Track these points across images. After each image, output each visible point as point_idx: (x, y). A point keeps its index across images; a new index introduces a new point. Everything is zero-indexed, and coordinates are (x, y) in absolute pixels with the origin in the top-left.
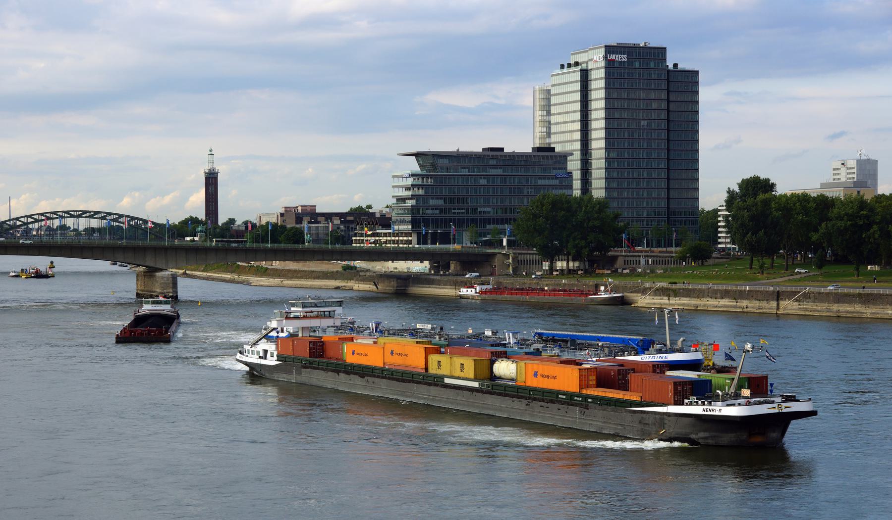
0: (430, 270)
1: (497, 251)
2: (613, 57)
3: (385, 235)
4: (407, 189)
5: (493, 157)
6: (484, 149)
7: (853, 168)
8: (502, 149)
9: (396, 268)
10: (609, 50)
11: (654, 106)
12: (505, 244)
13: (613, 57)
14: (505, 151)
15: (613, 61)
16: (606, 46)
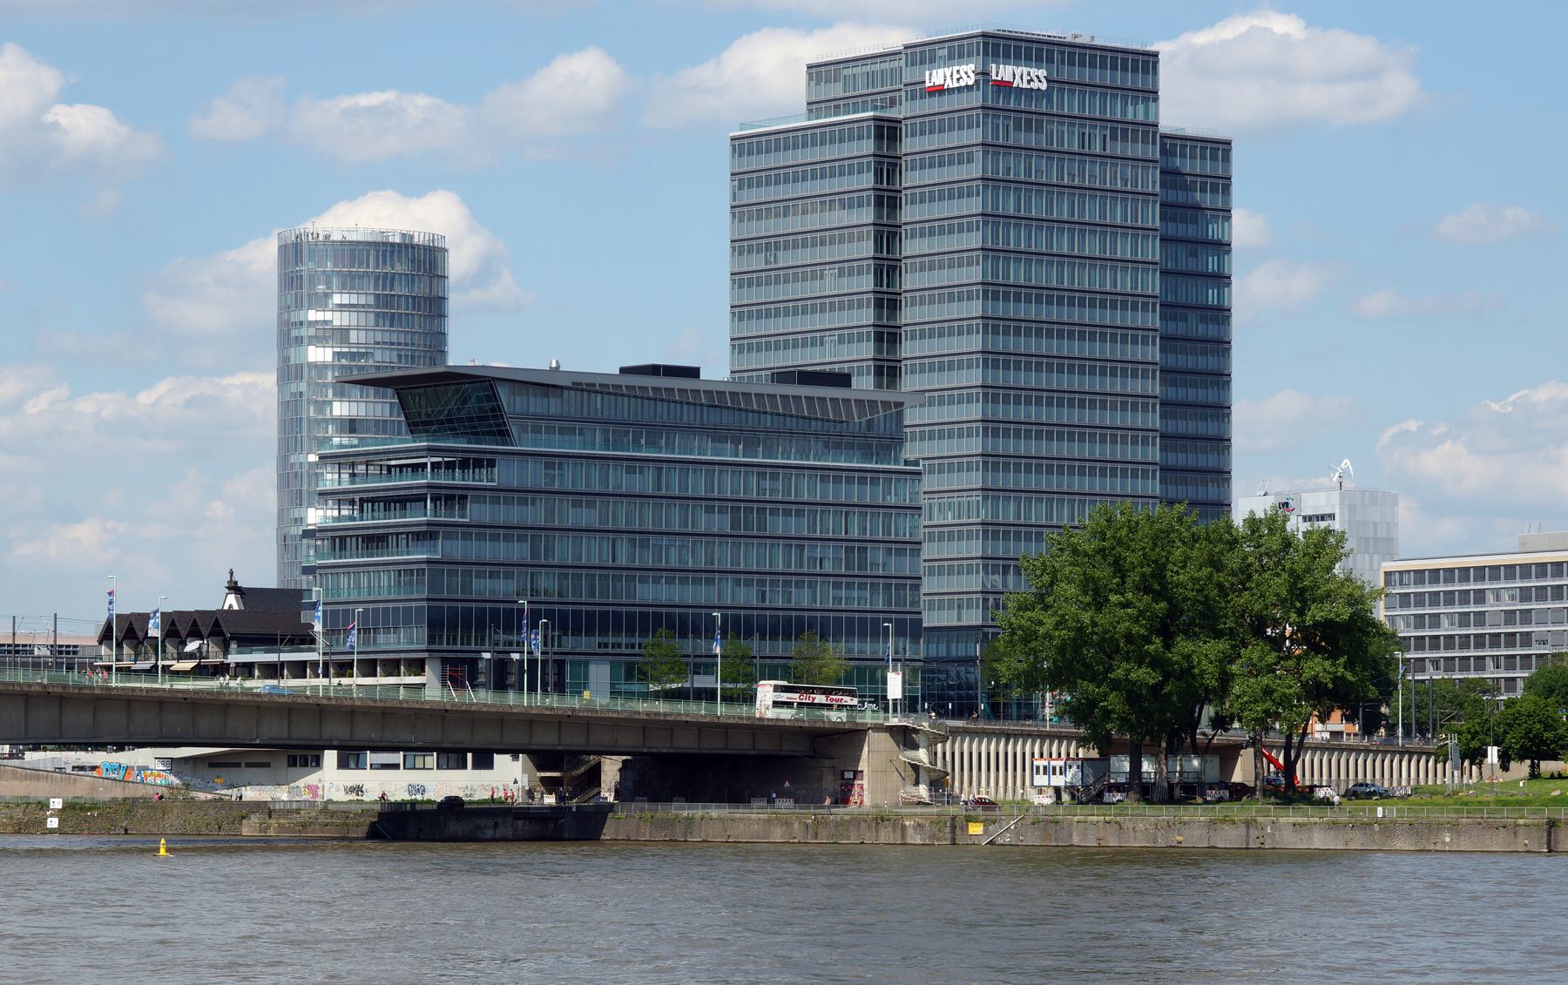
0: (530, 793)
1: (868, 717)
2: (1005, 72)
3: (272, 670)
4: (368, 501)
5: (659, 396)
6: (624, 370)
7: (1332, 517)
8: (693, 373)
9: (358, 790)
10: (998, 45)
11: (1123, 249)
12: (895, 686)
13: (1005, 72)
14: (703, 376)
15: (1004, 87)
16: (984, 35)
